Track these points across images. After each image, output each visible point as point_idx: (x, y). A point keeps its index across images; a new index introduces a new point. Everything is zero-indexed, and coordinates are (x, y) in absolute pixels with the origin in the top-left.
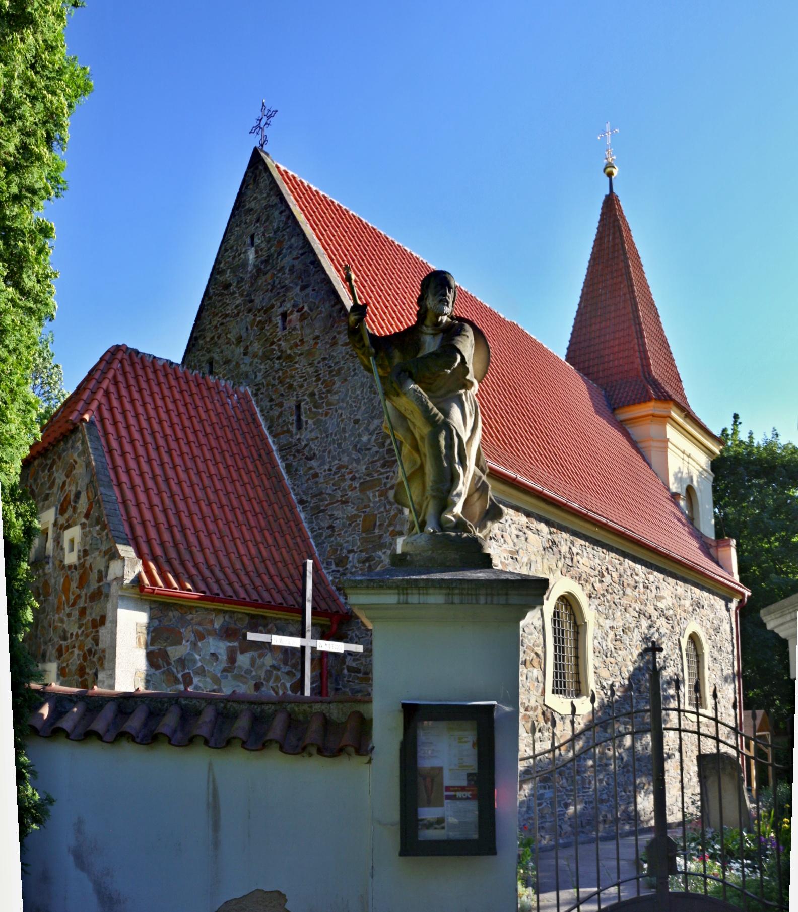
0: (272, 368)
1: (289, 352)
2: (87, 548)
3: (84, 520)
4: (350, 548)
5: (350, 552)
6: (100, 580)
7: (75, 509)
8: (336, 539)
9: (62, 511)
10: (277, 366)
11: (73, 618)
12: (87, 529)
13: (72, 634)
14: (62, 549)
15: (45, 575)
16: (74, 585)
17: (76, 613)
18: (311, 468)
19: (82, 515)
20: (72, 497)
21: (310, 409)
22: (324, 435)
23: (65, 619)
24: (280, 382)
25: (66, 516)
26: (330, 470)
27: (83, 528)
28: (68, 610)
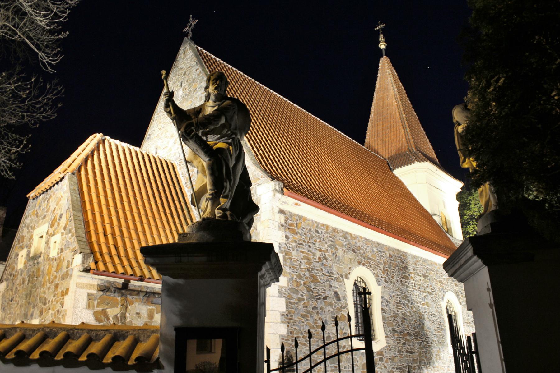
2: (63, 247)
3: (63, 231)
6: (67, 267)
7: (59, 224)
9: (52, 225)
11: (51, 291)
12: (64, 236)
13: (49, 301)
14: (49, 248)
15: (38, 263)
16: (54, 269)
17: (53, 287)
19: (62, 228)
20: (58, 217)
23: (47, 291)
25: (54, 228)
27: (62, 235)
28: (48, 285)
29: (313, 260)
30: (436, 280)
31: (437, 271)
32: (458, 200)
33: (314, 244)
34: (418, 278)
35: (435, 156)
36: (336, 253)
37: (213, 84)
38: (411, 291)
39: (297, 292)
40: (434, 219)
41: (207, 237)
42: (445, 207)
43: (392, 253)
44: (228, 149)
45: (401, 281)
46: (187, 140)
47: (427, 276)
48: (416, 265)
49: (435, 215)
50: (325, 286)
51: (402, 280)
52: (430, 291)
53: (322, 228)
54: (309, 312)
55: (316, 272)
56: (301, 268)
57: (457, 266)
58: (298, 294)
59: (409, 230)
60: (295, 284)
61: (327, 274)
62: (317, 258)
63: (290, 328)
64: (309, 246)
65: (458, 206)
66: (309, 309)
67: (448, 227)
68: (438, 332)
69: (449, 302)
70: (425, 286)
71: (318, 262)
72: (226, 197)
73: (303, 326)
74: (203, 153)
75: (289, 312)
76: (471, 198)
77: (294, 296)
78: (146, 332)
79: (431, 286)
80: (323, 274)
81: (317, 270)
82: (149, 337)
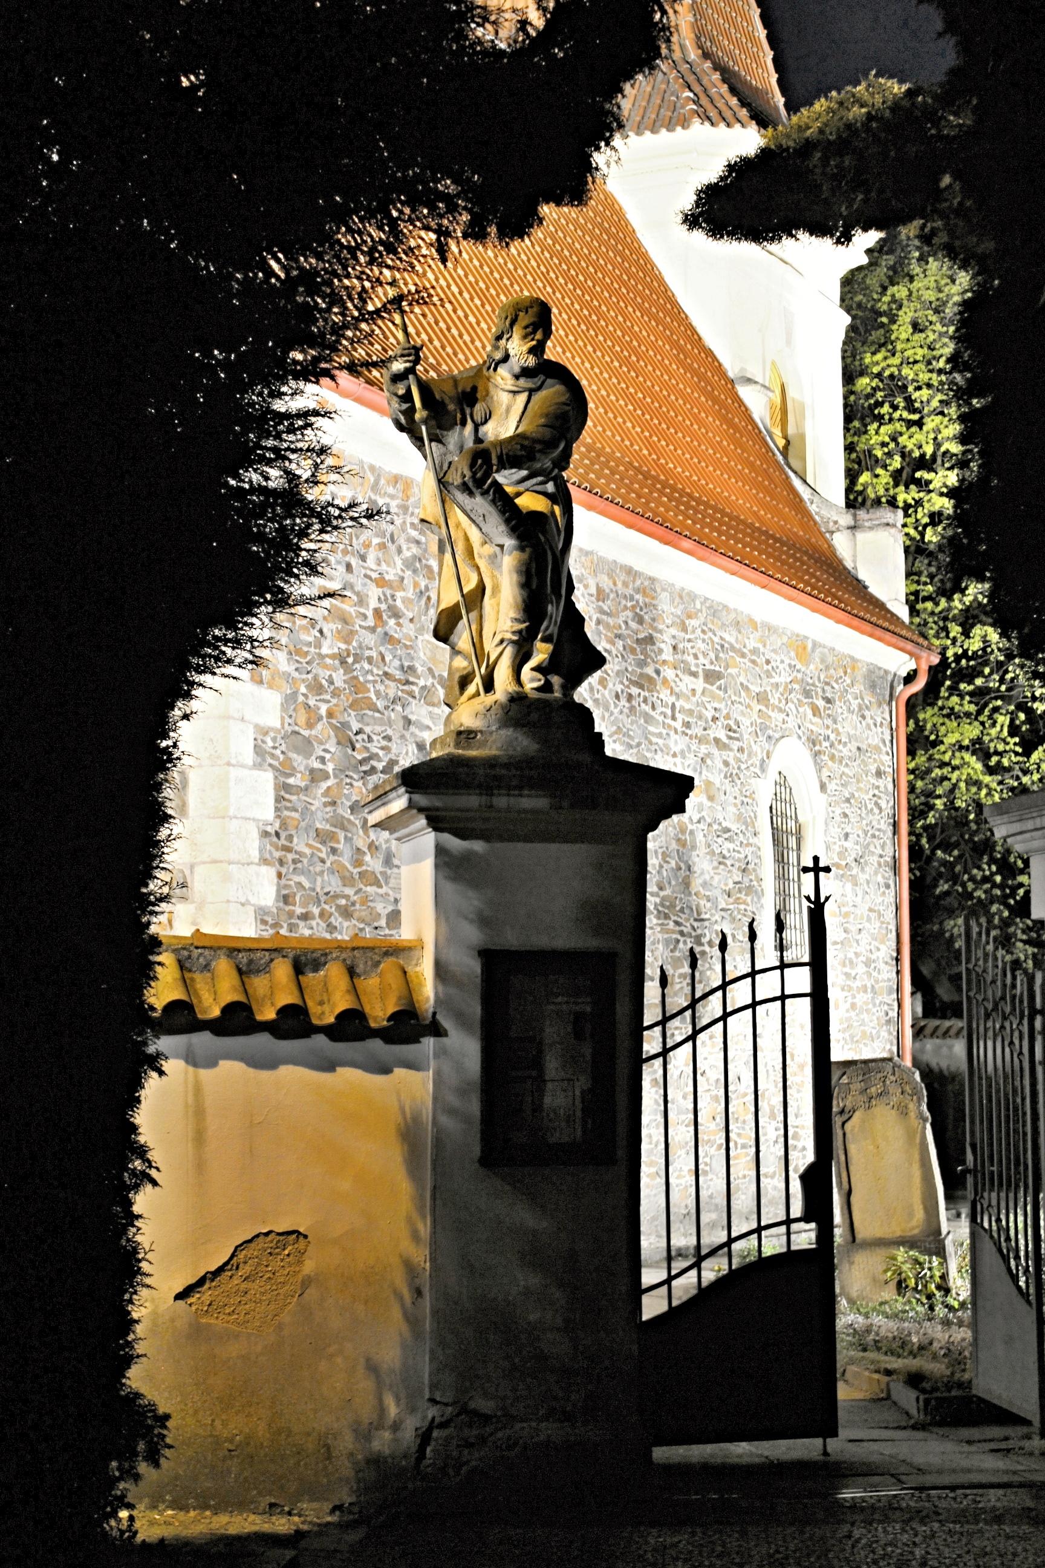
29: (359, 622)
30: (747, 689)
31: (755, 651)
32: (846, 303)
33: (363, 558)
34: (687, 683)
35: (774, 77)
36: (427, 589)
37: (525, 337)
38: (660, 735)
39: (306, 746)
40: (741, 403)
41: (524, 743)
42: (789, 342)
43: (606, 583)
44: (553, 513)
45: (630, 697)
46: (471, 494)
47: (718, 676)
48: (685, 629)
49: (749, 381)
50: (390, 723)
51: (635, 691)
52: (722, 735)
53: (391, 490)
54: (341, 824)
55: (367, 666)
56: (319, 655)
57: (1030, 825)
58: (308, 755)
59: (662, 468)
60: (302, 718)
61: (398, 674)
62: (370, 614)
63: (283, 882)
64: (349, 567)
65: (842, 336)
66: (340, 811)
67: (791, 430)
68: (737, 901)
69: (782, 781)
70: (709, 714)
71: (373, 630)
72: (546, 639)
73: (322, 873)
74: (503, 528)
75: (284, 825)
76: (900, 291)
77: (298, 760)
78: (370, 954)
79: (727, 717)
80: (386, 674)
81: (370, 660)
82: (377, 964)
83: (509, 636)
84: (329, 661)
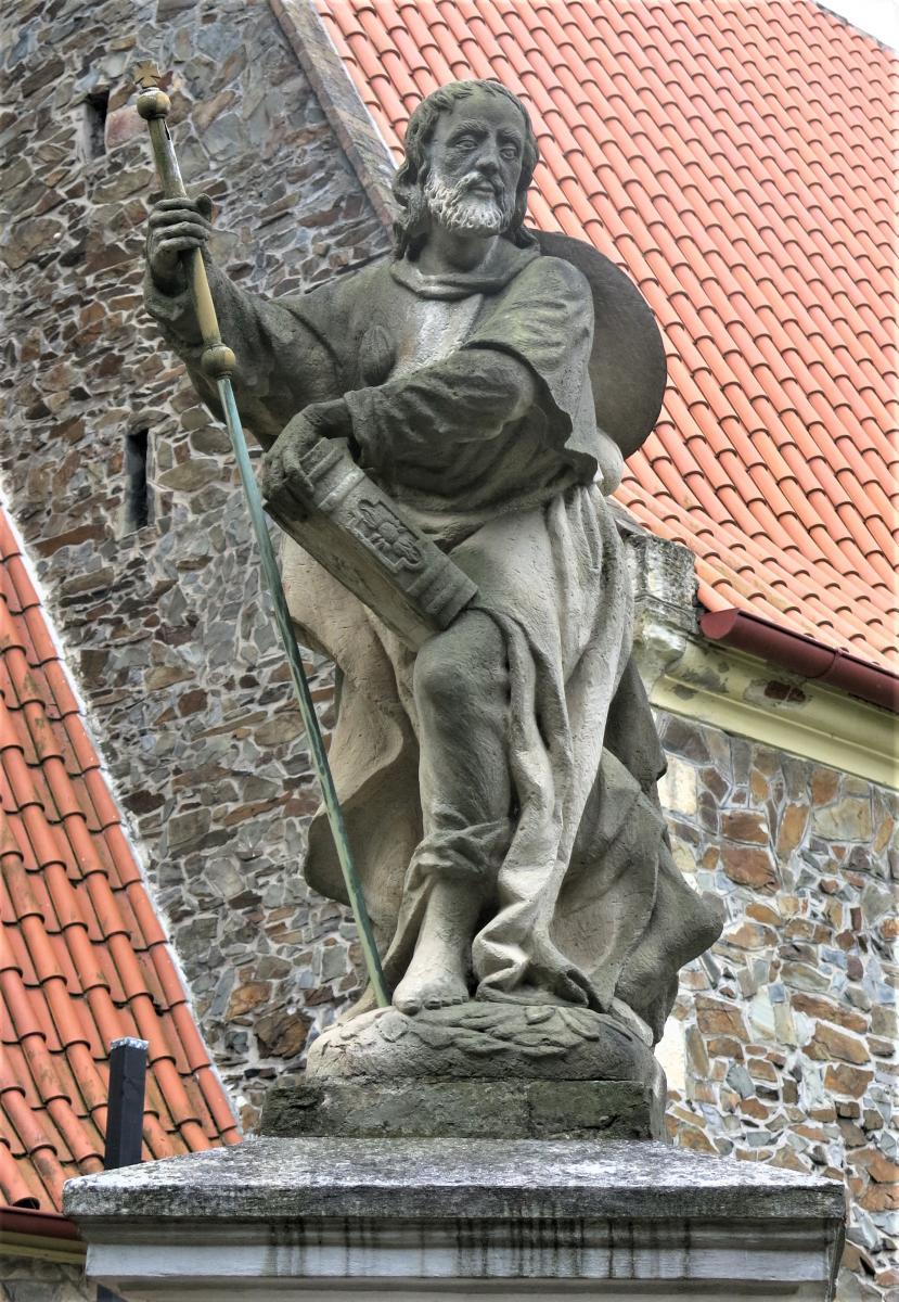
0: (45, 294)
1: (110, 238)
4: (317, 984)
5: (314, 998)
8: (264, 948)
10: (64, 289)
18: (177, 673)
21: (182, 454)
22: (230, 551)
24: (76, 347)
26: (249, 682)
83: (428, 859)
84: (812, 1124)
